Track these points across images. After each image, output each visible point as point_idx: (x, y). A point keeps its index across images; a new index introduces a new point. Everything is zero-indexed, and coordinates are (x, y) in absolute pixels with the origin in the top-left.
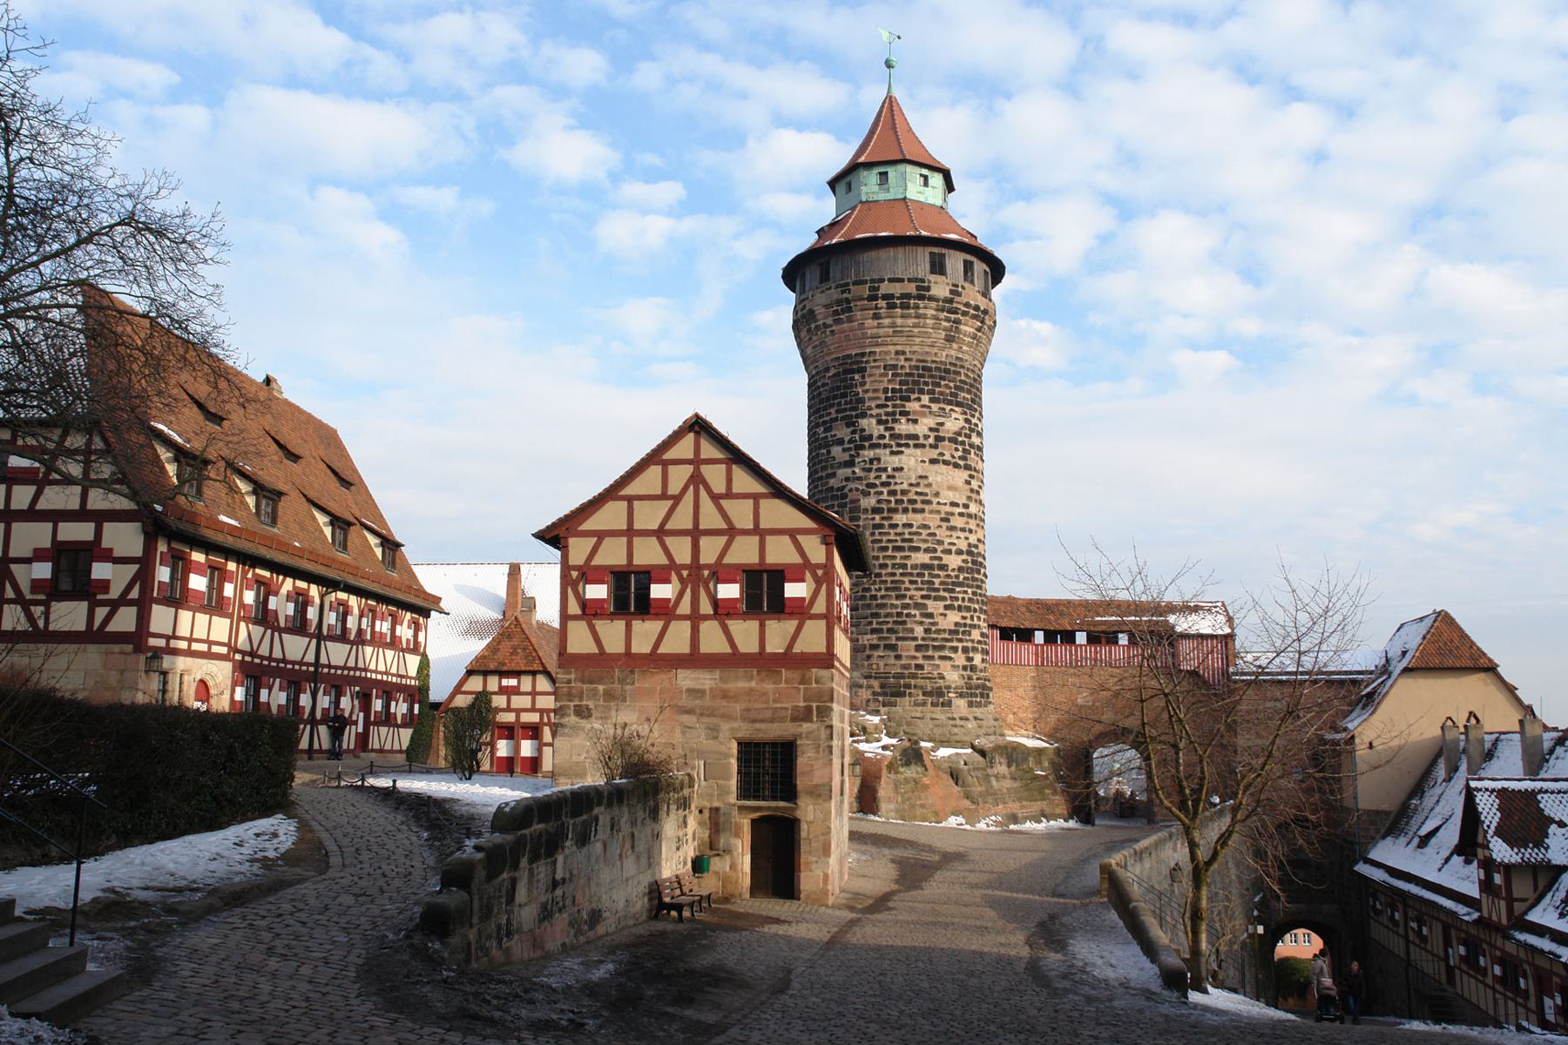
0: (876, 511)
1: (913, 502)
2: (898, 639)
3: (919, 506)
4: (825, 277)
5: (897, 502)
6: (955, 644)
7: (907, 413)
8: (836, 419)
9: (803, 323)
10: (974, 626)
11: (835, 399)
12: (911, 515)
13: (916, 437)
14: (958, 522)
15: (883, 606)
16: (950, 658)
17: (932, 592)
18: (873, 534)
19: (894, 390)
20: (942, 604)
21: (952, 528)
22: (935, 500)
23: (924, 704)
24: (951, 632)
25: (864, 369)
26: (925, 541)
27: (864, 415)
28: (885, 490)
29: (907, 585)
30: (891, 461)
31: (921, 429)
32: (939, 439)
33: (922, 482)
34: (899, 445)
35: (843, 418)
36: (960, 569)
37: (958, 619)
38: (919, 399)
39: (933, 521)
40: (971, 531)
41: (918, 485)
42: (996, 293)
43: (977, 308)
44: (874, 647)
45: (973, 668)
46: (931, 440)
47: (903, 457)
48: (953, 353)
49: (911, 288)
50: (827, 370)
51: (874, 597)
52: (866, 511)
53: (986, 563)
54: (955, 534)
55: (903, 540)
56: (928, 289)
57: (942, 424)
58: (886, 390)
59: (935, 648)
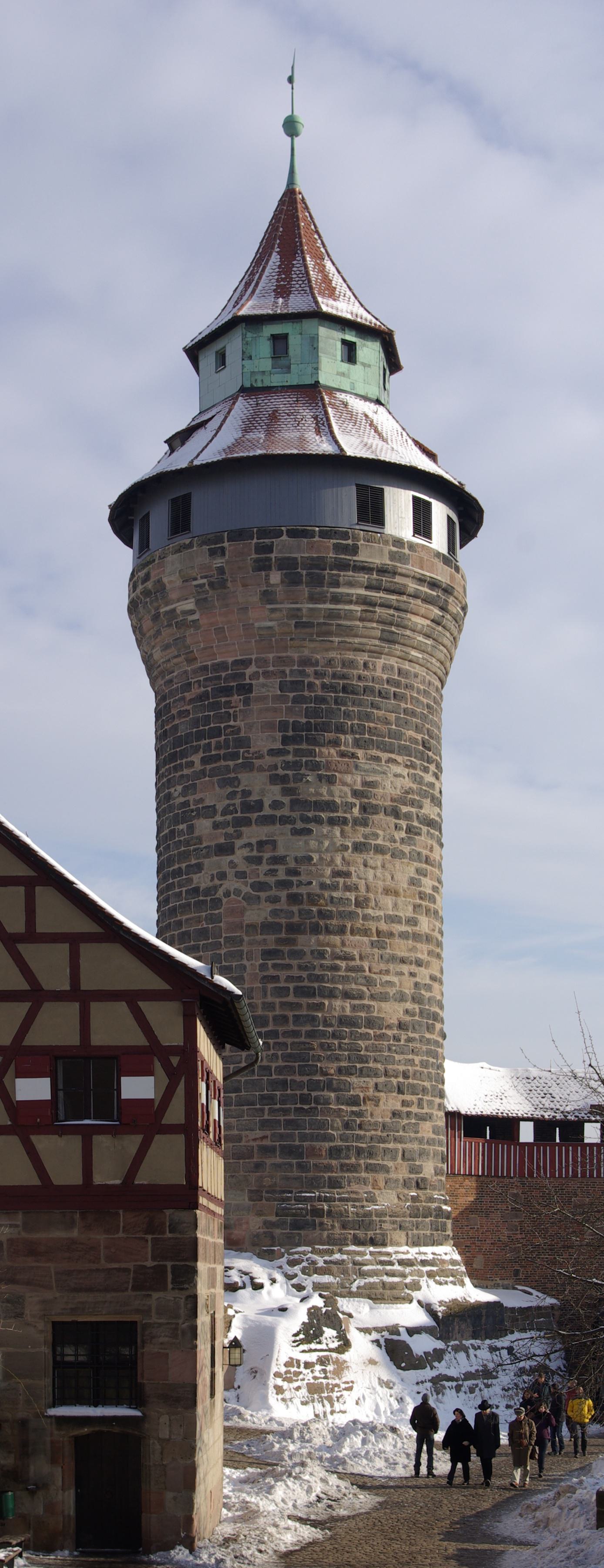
0: (267, 927)
2: (303, 1137)
4: (180, 522)
6: (391, 1146)
8: (203, 773)
9: (147, 605)
11: (193, 734)
14: (400, 947)
15: (284, 1084)
16: (387, 1170)
18: (263, 967)
20: (371, 1082)
24: (384, 1126)
25: (249, 689)
27: (248, 766)
28: (283, 894)
31: (340, 793)
33: (341, 880)
35: (213, 773)
37: (398, 1107)
39: (356, 944)
41: (335, 887)
42: (465, 555)
48: (393, 662)
50: (188, 687)
53: (445, 1014)
55: (312, 978)
58: (283, 726)
59: (359, 1152)
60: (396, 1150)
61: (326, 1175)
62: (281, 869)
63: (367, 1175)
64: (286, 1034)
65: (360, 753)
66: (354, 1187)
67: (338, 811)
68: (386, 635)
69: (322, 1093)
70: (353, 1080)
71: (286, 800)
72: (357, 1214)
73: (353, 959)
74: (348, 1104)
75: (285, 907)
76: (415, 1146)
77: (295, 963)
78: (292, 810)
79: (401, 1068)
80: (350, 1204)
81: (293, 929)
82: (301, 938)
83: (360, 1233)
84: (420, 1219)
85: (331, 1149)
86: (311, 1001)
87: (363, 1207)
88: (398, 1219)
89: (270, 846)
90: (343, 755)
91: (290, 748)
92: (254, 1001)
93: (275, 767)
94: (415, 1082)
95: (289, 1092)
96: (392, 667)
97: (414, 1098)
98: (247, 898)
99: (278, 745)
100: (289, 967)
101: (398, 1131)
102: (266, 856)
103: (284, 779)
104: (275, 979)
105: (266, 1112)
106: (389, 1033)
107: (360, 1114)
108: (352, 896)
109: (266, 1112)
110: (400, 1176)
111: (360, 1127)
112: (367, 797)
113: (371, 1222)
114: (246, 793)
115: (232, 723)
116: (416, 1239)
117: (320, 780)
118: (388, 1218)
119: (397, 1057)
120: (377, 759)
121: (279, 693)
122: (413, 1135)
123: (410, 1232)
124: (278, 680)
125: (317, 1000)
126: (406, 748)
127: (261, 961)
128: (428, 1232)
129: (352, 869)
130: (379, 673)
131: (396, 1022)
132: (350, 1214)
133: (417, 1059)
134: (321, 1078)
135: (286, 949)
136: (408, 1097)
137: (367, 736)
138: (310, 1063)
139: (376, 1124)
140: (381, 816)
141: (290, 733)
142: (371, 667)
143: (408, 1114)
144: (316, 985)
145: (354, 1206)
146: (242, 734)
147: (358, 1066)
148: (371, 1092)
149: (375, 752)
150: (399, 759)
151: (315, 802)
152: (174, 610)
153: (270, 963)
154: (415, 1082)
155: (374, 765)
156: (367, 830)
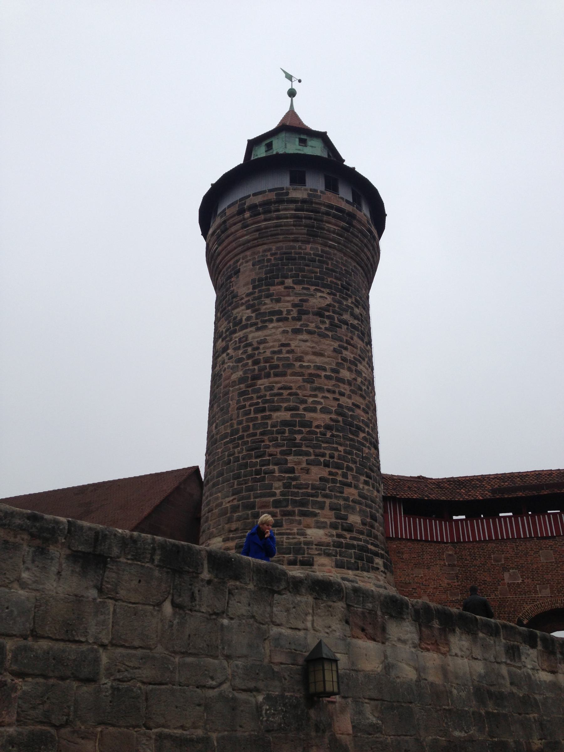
0: (242, 380)
3: (281, 369)
5: (260, 370)
6: (320, 499)
7: (272, 295)
10: (349, 485)
12: (272, 379)
13: (280, 312)
15: (245, 466)
16: (315, 515)
17: (293, 447)
18: (238, 402)
19: (260, 280)
20: (305, 458)
21: (320, 389)
24: (314, 487)
25: (239, 271)
26: (288, 400)
28: (250, 362)
30: (254, 336)
31: (284, 306)
32: (302, 312)
33: (284, 349)
36: (328, 427)
38: (282, 283)
40: (342, 394)
41: (280, 352)
44: (235, 509)
45: (350, 529)
46: (295, 313)
49: (272, 196)
51: (237, 459)
52: (234, 383)
54: (320, 395)
56: (287, 194)
57: (306, 301)
58: (253, 281)
59: (295, 503)
62: (249, 349)
63: (300, 518)
65: (295, 286)
67: (282, 315)
70: (289, 458)
71: (254, 315)
73: (290, 388)
74: (286, 472)
76: (342, 502)
77: (255, 396)
78: (257, 319)
79: (328, 452)
80: (285, 537)
81: (256, 378)
82: (260, 382)
84: (343, 550)
85: (274, 501)
89: (244, 339)
91: (257, 290)
93: (249, 301)
94: (339, 461)
95: (249, 469)
96: (317, 248)
97: (340, 472)
98: (233, 368)
99: (251, 290)
100: (252, 398)
101: (324, 490)
102: (242, 344)
104: (244, 406)
105: (236, 484)
106: (318, 430)
109: (236, 484)
113: (300, 549)
114: (235, 318)
115: (232, 289)
117: (272, 301)
118: (314, 547)
119: (323, 445)
120: (308, 289)
123: (334, 558)
125: (268, 413)
128: (353, 561)
130: (308, 250)
131: (323, 424)
132: (284, 544)
135: (250, 389)
136: (334, 470)
138: (262, 450)
141: (257, 283)
142: (303, 247)
143: (334, 481)
144: (266, 405)
145: (288, 538)
146: (235, 292)
147: (294, 449)
148: (304, 465)
150: (322, 289)
151: (269, 312)
153: (241, 398)
154: (339, 461)
155: (305, 292)
156: (300, 323)
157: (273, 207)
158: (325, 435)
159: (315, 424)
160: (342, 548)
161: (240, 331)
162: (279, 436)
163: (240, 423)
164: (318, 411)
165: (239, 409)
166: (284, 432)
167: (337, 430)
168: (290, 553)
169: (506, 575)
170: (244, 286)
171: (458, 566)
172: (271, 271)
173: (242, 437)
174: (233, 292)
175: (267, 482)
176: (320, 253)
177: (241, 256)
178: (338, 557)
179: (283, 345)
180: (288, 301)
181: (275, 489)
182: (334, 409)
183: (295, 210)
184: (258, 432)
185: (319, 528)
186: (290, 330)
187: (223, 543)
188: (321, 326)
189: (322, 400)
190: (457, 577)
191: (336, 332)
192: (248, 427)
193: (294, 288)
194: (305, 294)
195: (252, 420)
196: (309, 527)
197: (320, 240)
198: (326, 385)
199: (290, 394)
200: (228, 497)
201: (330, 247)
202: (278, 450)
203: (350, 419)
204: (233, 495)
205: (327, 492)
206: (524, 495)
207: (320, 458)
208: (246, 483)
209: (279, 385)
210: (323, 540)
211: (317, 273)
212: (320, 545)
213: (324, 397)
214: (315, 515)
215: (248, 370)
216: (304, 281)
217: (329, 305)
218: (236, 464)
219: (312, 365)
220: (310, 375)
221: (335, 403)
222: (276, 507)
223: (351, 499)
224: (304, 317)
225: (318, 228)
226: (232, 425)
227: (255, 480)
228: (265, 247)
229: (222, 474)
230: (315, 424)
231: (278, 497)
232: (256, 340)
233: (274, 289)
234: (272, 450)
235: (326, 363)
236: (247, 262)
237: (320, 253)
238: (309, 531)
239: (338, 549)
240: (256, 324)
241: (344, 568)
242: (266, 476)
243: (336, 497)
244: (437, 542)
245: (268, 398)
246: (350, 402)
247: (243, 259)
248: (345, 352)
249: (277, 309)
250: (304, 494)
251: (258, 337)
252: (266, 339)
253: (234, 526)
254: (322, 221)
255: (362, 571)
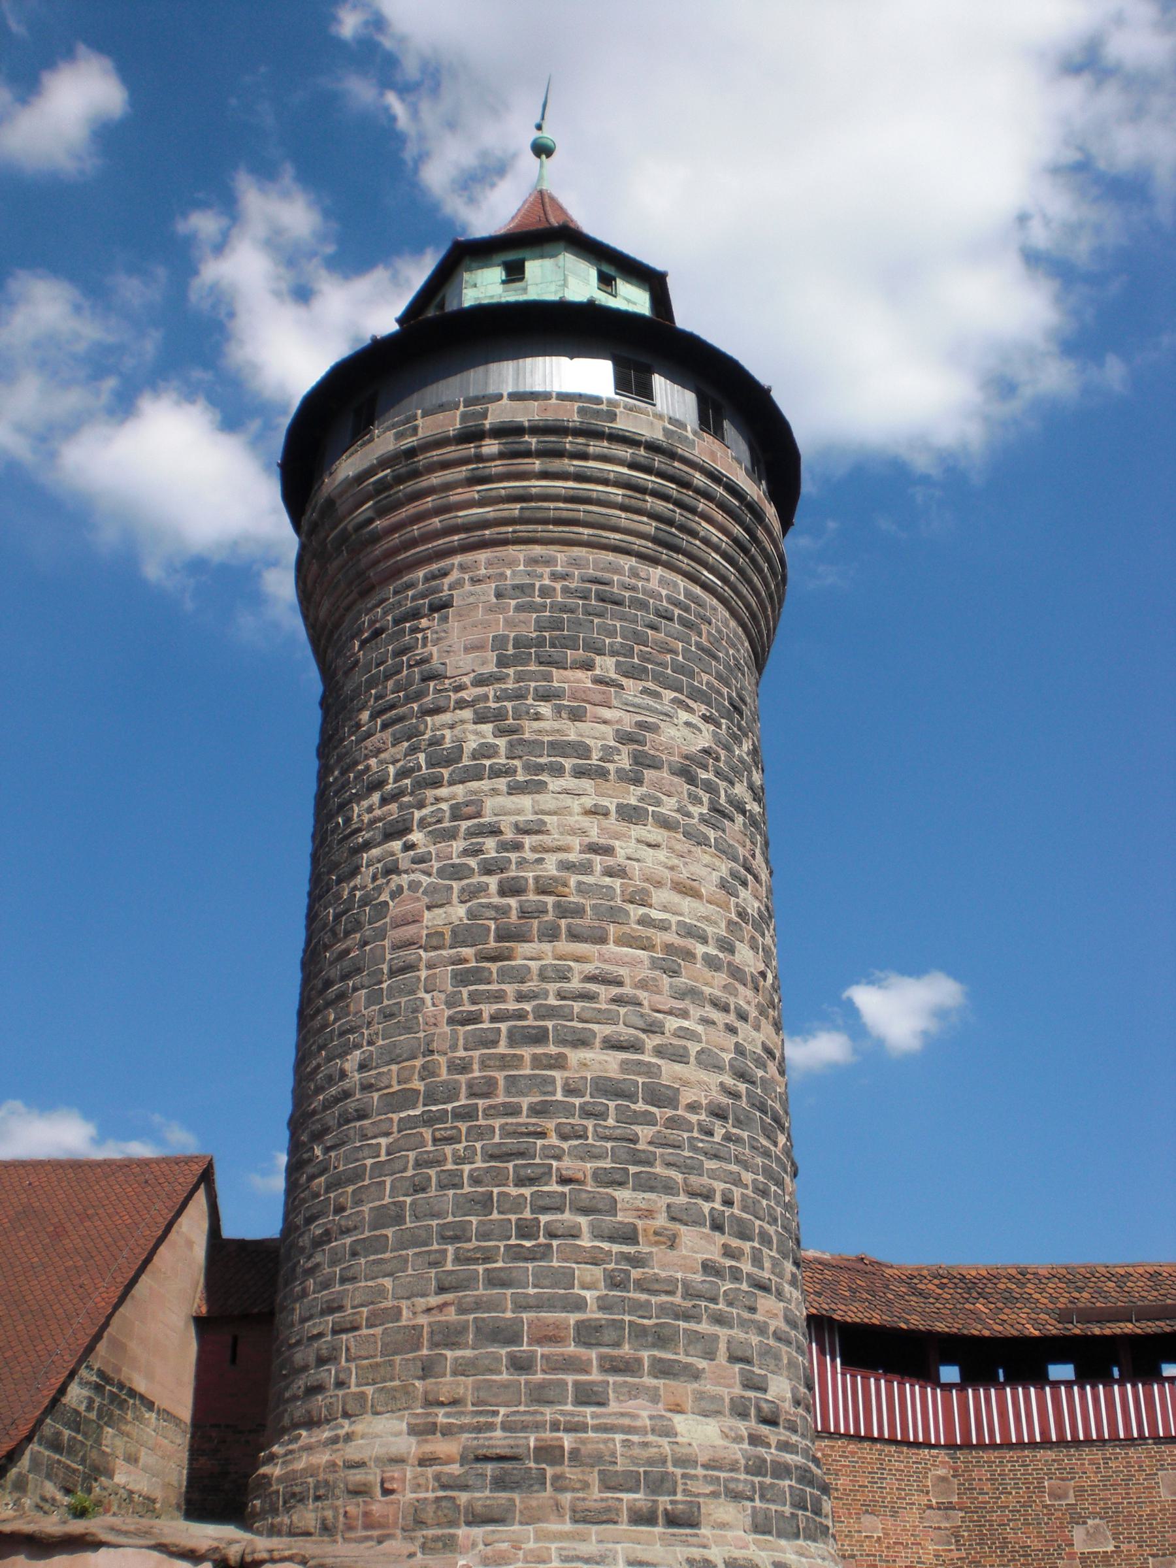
1: (563, 911)
3: (586, 922)
5: (524, 914)
6: (704, 1327)
12: (565, 946)
13: (582, 750)
15: (486, 1204)
16: (696, 1375)
17: (631, 1166)
18: (452, 1001)
21: (692, 993)
22: (636, 912)
23: (604, 1517)
26: (611, 1019)
28: (493, 882)
29: (553, 1140)
30: (504, 806)
31: (595, 734)
32: (643, 761)
34: (540, 769)
36: (719, 1114)
37: (714, 1254)
40: (743, 1017)
41: (586, 868)
43: (733, 489)
44: (449, 1337)
46: (624, 761)
47: (546, 801)
51: (452, 1181)
52: (435, 941)
54: (695, 1012)
56: (612, 417)
58: (499, 642)
59: (639, 1333)
60: (715, 1338)
61: (570, 1378)
62: (490, 843)
63: (655, 1382)
64: (490, 1112)
65: (625, 681)
66: (631, 1405)
67: (589, 758)
68: (661, 535)
69: (559, 1217)
70: (623, 1195)
72: (634, 1460)
74: (612, 1239)
75: (496, 900)
76: (755, 1339)
77: (510, 989)
80: (619, 1437)
83: (638, 1498)
85: (579, 1325)
86: (539, 1050)
87: (645, 1445)
88: (722, 1475)
90: (598, 681)
91: (511, 671)
92: (436, 1057)
93: (485, 697)
94: (745, 1215)
96: (676, 585)
97: (747, 1246)
98: (431, 890)
99: (491, 668)
100: (499, 997)
101: (714, 1300)
103: (498, 716)
104: (474, 1018)
106: (694, 1118)
107: (637, 1261)
108: (617, 883)
110: (725, 1392)
111: (641, 1286)
112: (637, 742)
113: (664, 1477)
114: (436, 742)
116: (760, 1518)
118: (700, 1471)
119: (711, 1165)
120: (656, 695)
121: (494, 600)
122: (746, 1315)
123: (748, 1504)
124: (493, 585)
125: (552, 1049)
126: (700, 690)
127: (450, 989)
129: (617, 843)
130: (653, 585)
131: (704, 1102)
133: (747, 1177)
134: (559, 1189)
135: (494, 967)
136: (735, 1243)
137: (636, 660)
138: (537, 1161)
139: (673, 1281)
140: (665, 774)
141: (511, 651)
142: (642, 574)
144: (550, 1024)
146: (435, 661)
147: (633, 1169)
148: (661, 1221)
149: (650, 685)
151: (551, 743)
152: (345, 529)
153: (465, 992)
154: (745, 1215)
155: (649, 701)
156: (643, 790)
157: (569, 443)
158: (710, 1133)
159: (688, 1096)
160: (765, 1476)
161: (452, 783)
162: (590, 1124)
163: (463, 1067)
164: (692, 1059)
165: (451, 1021)
166: (602, 1115)
167: (738, 1123)
168: (635, 1490)
169: (1078, 1534)
170: (467, 650)
171: (960, 1509)
172: (556, 625)
173: (467, 1114)
174: (424, 661)
175: (555, 1264)
176: (682, 598)
177: (457, 559)
178: (758, 1503)
179: (594, 849)
180: (605, 722)
181: (583, 1288)
182: (727, 1057)
183: (633, 466)
184: (525, 1102)
185: (705, 1414)
186: (613, 809)
187: (413, 1440)
188: (691, 808)
189: (700, 1029)
190: (957, 1536)
191: (724, 831)
192: (491, 1083)
193: (621, 687)
194: (649, 709)
195: (505, 1062)
196: (678, 1409)
197: (684, 562)
198: (706, 984)
199: (618, 1000)
200: (423, 1295)
201: (705, 586)
202: (589, 1166)
203: (759, 1091)
204: (442, 1290)
205: (721, 1306)
206: (1139, 1331)
207: (700, 1201)
208: (487, 1260)
209: (589, 968)
210: (722, 1454)
211: (675, 652)
212: (714, 1468)
213: (707, 1022)
214: (696, 1375)
215: (489, 906)
216: (645, 670)
217: (706, 751)
218: (451, 1192)
219: (674, 919)
220: (669, 948)
221: (730, 1041)
222: (588, 1345)
223: (772, 1329)
224: (649, 774)
225: (682, 528)
226: (428, 1071)
227: (517, 1254)
228: (538, 550)
229: (399, 1219)
230: (688, 1096)
231: (593, 1314)
232: (513, 819)
233: (560, 679)
234: (568, 1165)
235: (707, 919)
236: (475, 581)
237: (682, 598)
238: (680, 1422)
239: (757, 1479)
240: (509, 772)
241: (769, 1533)
242: (555, 1243)
243: (744, 1324)
244: (916, 1445)
245: (552, 1001)
246: (760, 1037)
247: (463, 568)
248: (743, 893)
249: (572, 737)
250: (663, 1309)
251: (519, 812)
252: (544, 823)
253: (447, 1385)
254: (693, 510)
255: (806, 1538)
